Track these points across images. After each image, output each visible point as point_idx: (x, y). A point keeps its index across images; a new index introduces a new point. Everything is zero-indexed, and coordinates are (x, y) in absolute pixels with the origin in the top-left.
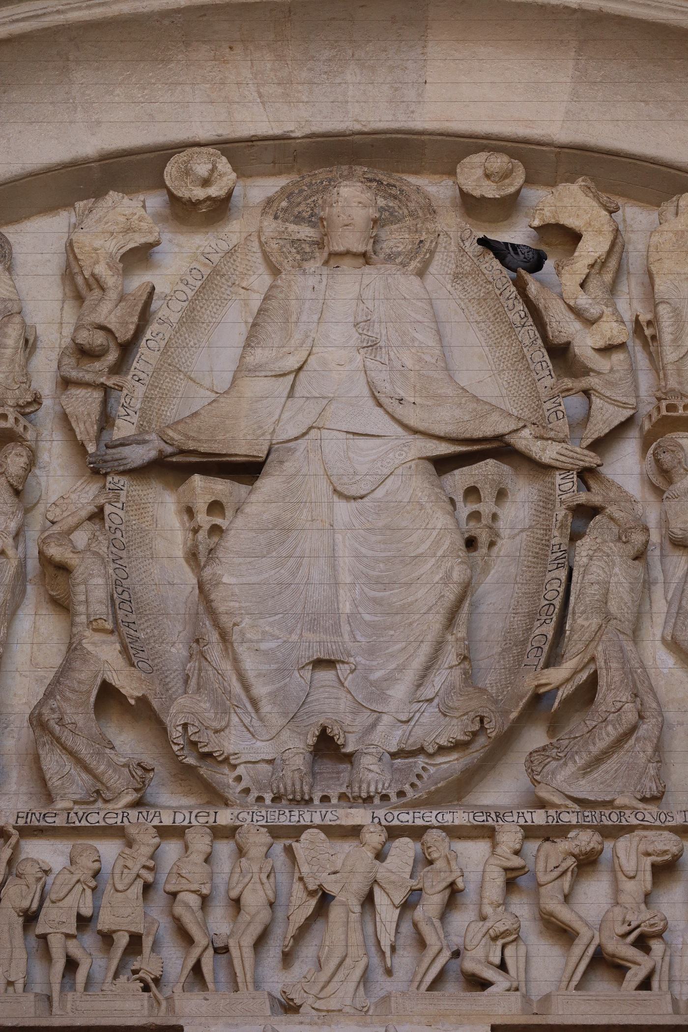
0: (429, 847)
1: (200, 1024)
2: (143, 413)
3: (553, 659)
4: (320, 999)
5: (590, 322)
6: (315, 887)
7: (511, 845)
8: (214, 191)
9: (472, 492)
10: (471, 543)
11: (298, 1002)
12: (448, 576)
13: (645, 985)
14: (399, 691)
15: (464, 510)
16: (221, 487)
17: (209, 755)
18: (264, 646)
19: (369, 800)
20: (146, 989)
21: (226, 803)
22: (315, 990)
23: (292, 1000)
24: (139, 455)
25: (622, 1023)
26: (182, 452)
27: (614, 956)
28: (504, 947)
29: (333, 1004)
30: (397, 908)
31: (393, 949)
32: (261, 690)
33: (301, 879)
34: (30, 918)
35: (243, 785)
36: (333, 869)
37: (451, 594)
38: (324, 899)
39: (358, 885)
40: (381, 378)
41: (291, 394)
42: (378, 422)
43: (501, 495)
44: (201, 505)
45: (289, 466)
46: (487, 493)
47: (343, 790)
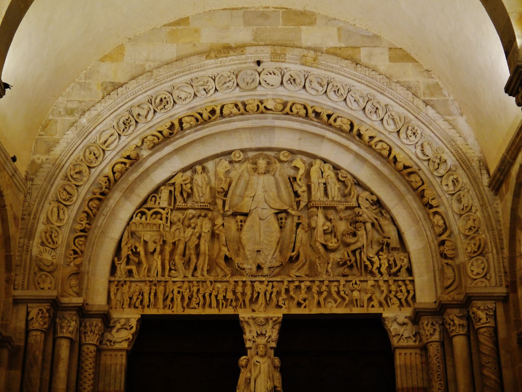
2: (230, 205)
3: (293, 251)
5: (301, 187)
8: (240, 159)
9: (281, 219)
10: (281, 227)
12: (277, 236)
13: (305, 307)
14: (270, 257)
15: (280, 221)
16: (242, 218)
17: (241, 269)
18: (250, 248)
19: (265, 276)
20: (233, 308)
21: (244, 276)
24: (229, 213)
26: (235, 212)
29: (260, 311)
32: (249, 257)
34: (216, 296)
35: (247, 273)
37: (277, 240)
38: (259, 293)
39: (264, 290)
40: (267, 197)
41: (253, 200)
42: (266, 206)
43: (286, 219)
44: (239, 221)
45: (253, 215)
46: (284, 218)
47: (261, 274)
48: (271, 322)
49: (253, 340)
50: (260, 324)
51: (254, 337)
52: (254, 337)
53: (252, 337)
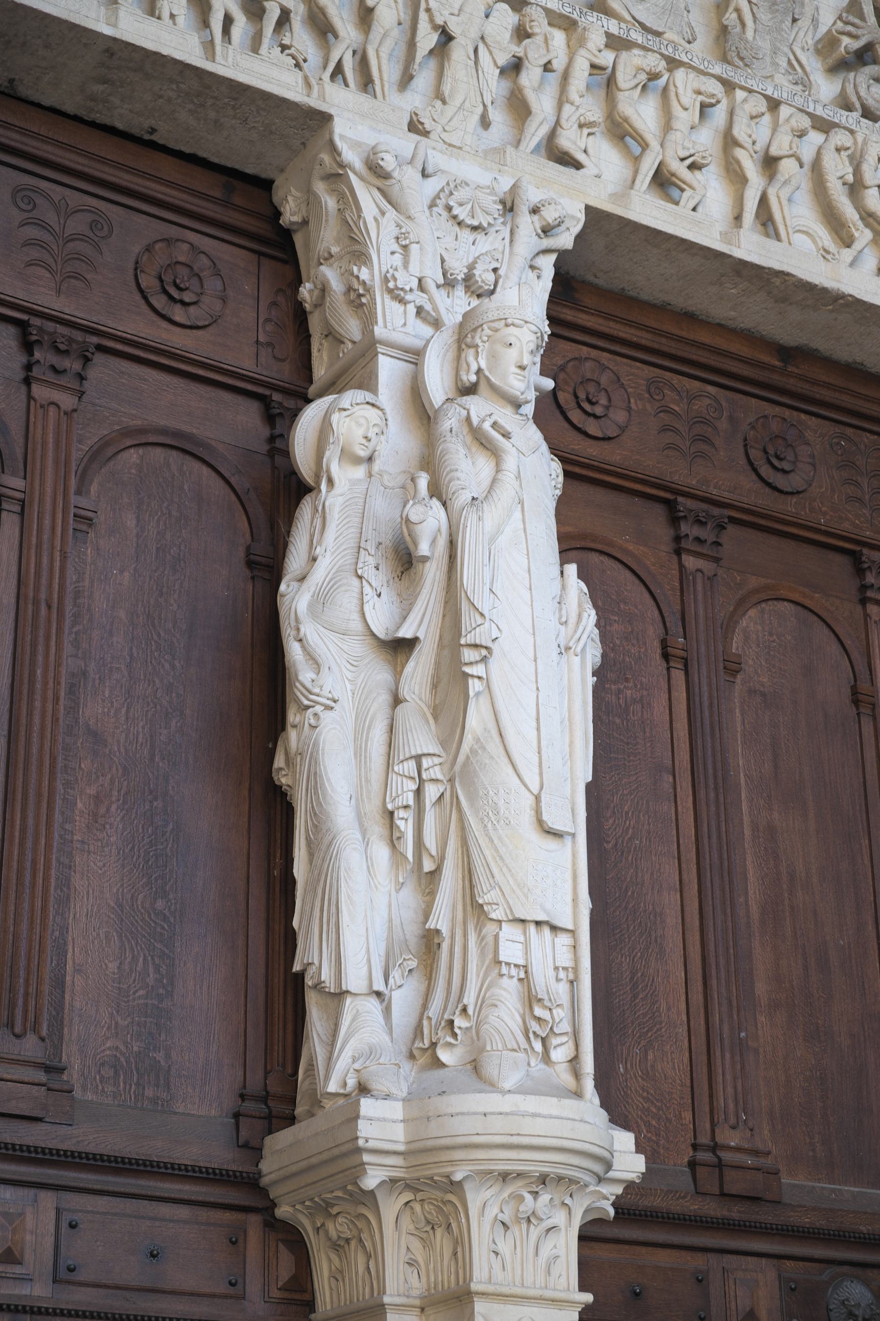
0: (533, 21)
1: (349, 119)
4: (445, 130)
6: (442, 23)
7: (598, 44)
11: (428, 127)
22: (444, 121)
23: (422, 124)
25: (684, 237)
27: (673, 175)
28: (589, 134)
30: (498, 67)
31: (492, 103)
33: (428, 10)
36: (451, 11)
39: (474, 33)
48: (527, 225)
49: (420, 298)
50: (462, 213)
51: (421, 287)
52: (421, 287)
53: (415, 284)
